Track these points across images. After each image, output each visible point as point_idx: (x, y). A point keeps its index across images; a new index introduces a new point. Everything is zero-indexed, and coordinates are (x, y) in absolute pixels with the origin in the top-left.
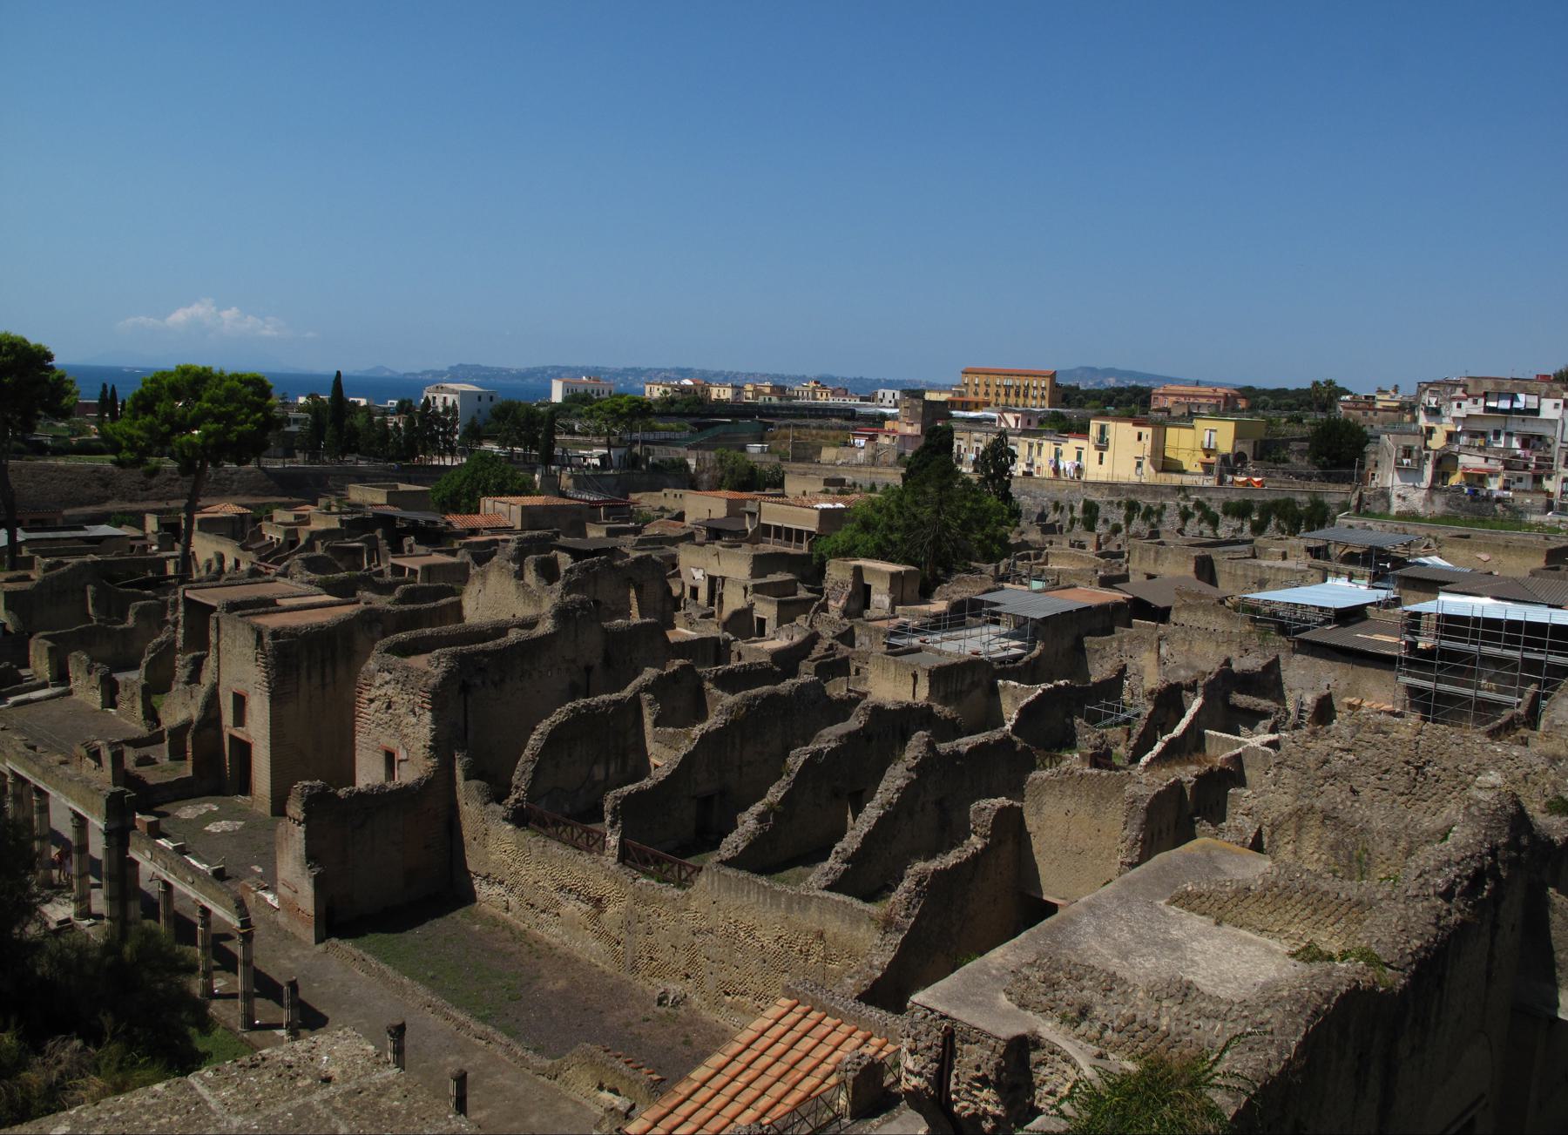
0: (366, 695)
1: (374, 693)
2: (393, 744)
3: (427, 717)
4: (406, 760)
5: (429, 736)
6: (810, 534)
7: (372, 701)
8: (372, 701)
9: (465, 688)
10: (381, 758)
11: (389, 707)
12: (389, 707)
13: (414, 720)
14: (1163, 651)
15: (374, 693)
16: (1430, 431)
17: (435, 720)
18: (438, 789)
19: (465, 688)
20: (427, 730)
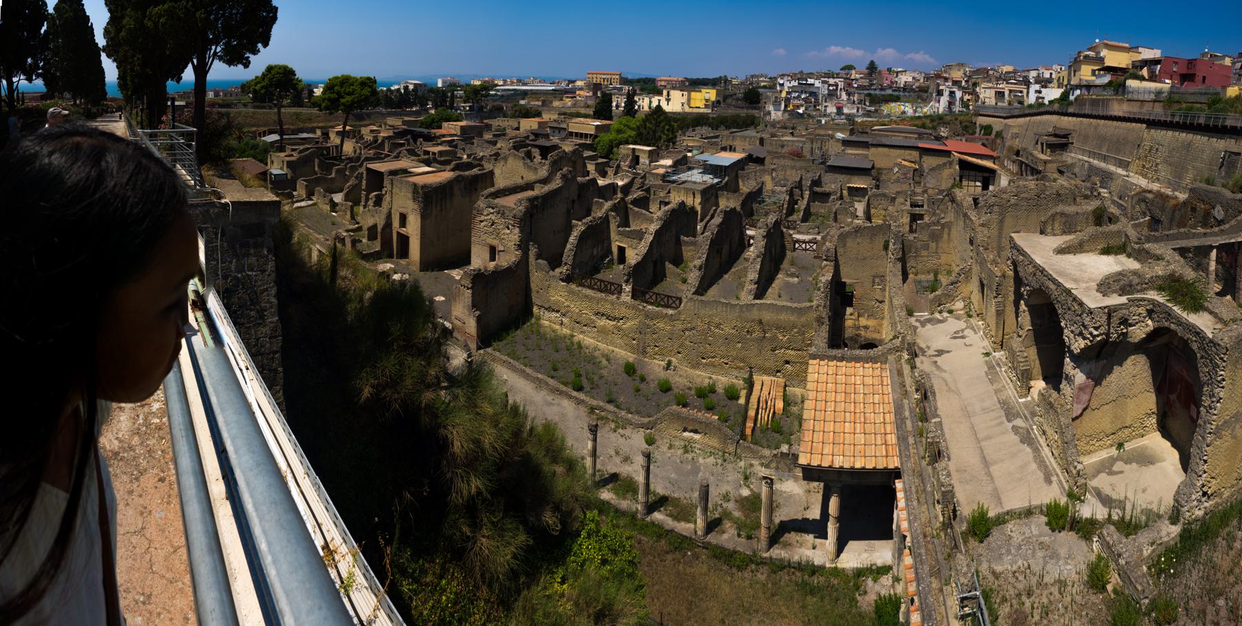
0: (478, 219)
1: (483, 218)
2: (495, 242)
3: (517, 230)
4: (503, 251)
5: (518, 239)
6: (591, 135)
7: (482, 221)
8: (482, 221)
9: (531, 216)
10: (487, 249)
11: (492, 225)
12: (492, 225)
13: (508, 231)
14: (774, 175)
15: (483, 218)
16: (781, 91)
17: (521, 232)
18: (523, 263)
19: (531, 216)
20: (516, 237)
